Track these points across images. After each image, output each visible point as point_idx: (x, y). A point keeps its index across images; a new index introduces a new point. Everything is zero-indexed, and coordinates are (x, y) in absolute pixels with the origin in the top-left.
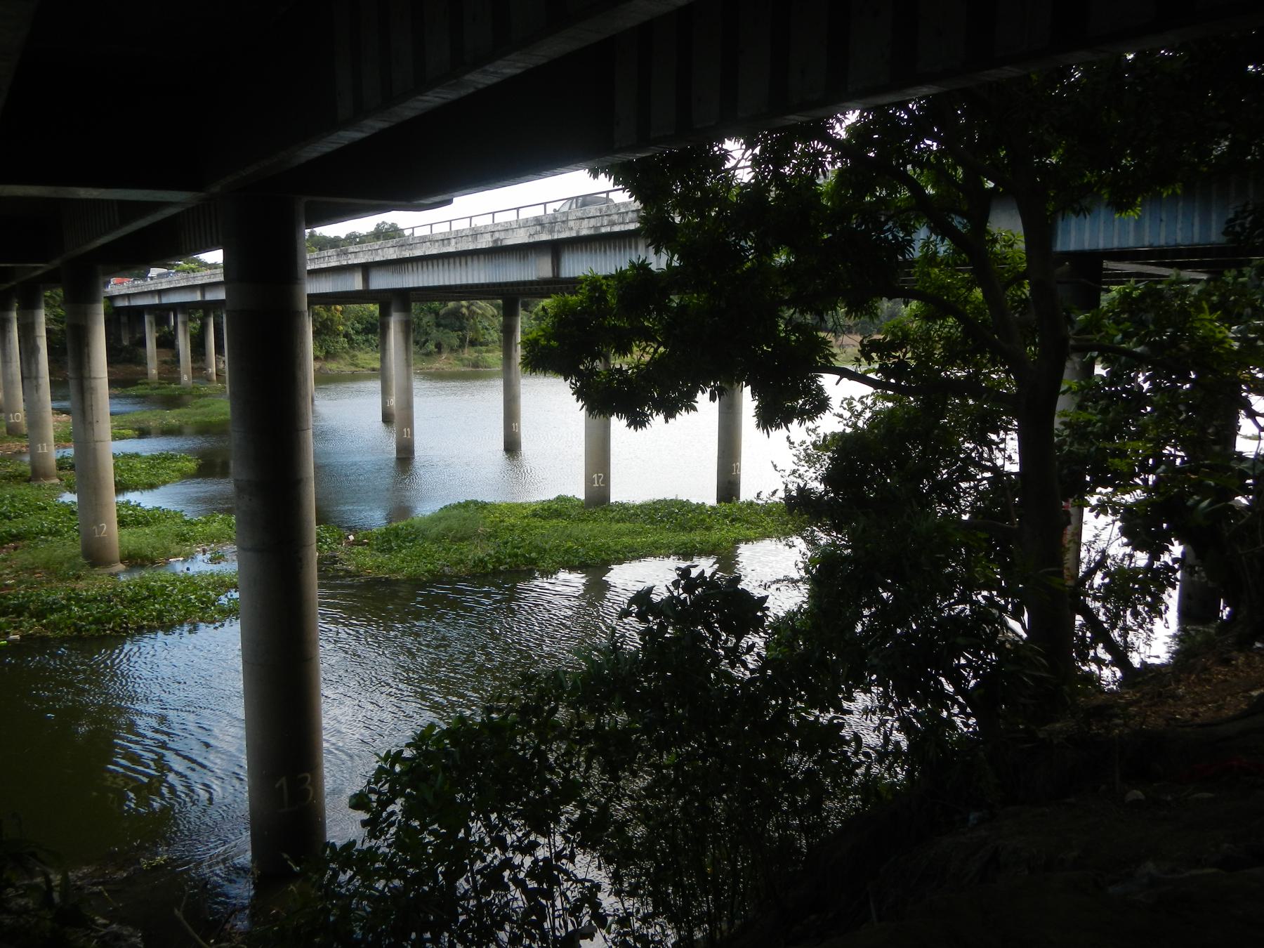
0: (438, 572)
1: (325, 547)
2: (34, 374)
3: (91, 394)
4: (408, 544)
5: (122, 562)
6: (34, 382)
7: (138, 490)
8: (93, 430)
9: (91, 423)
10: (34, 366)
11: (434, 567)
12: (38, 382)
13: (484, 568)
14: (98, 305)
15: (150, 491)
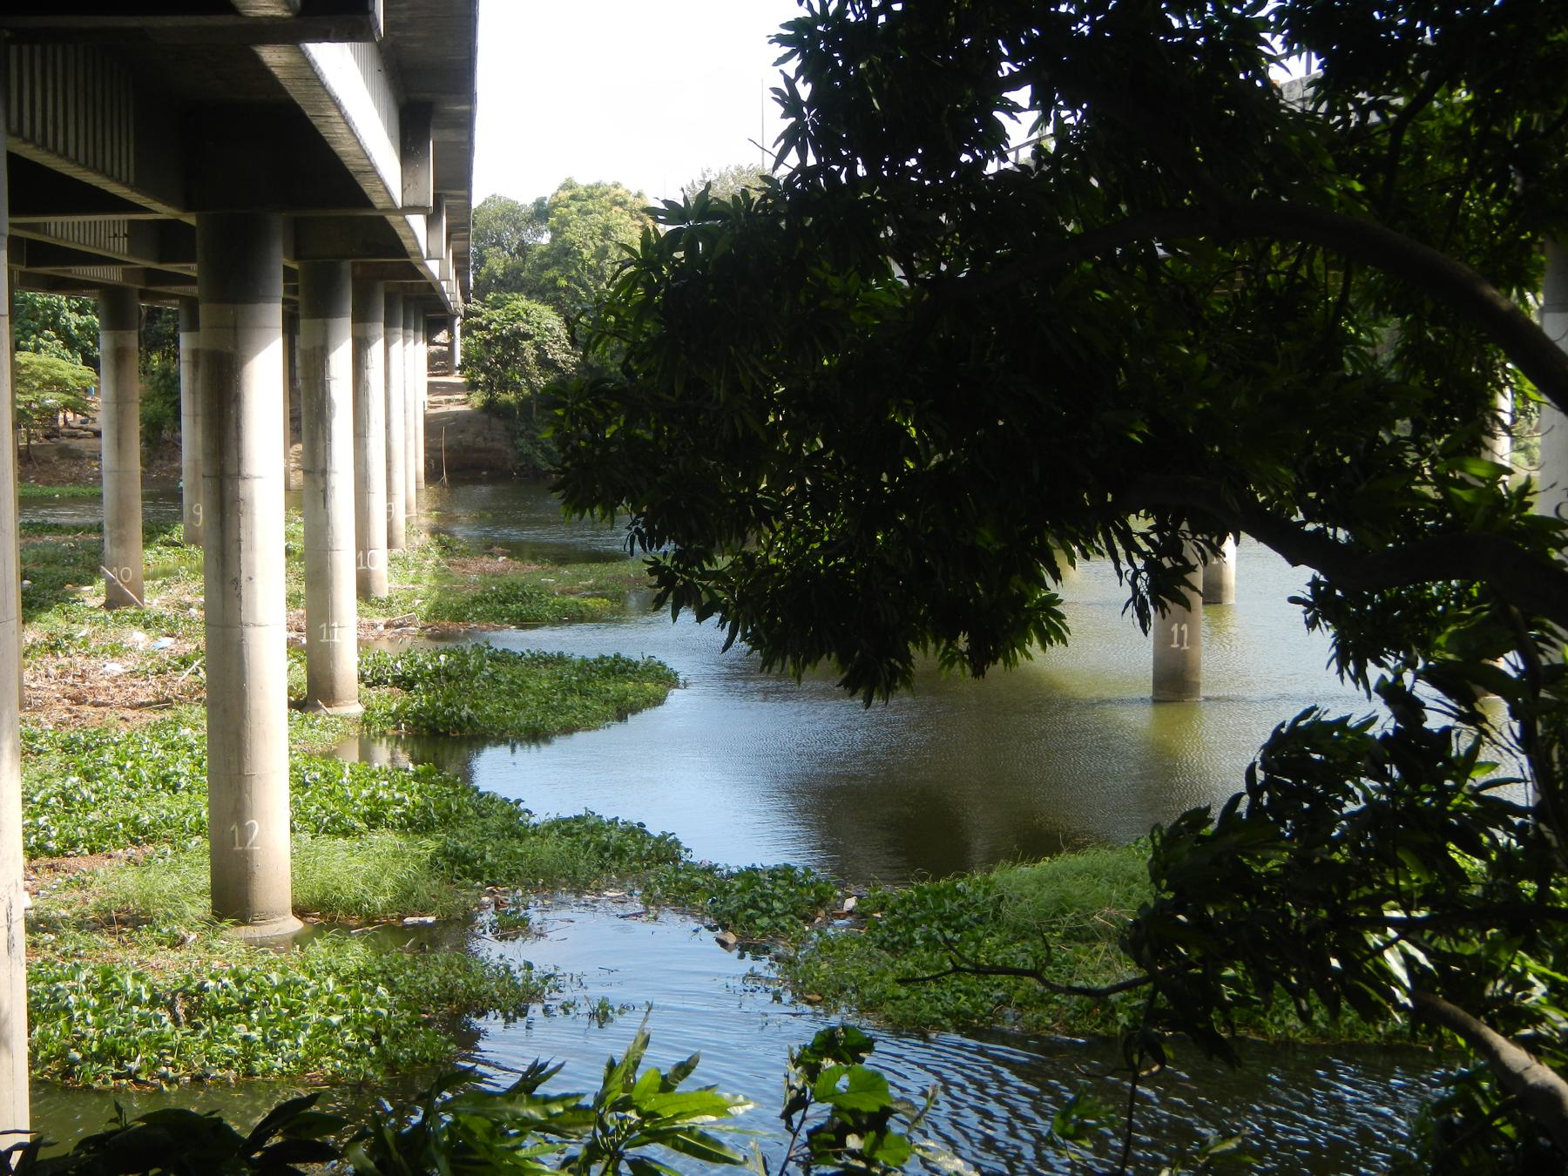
0: (981, 1019)
1: (764, 921)
2: (321, 466)
3: (238, 513)
4: (949, 934)
5: (300, 911)
6: (321, 481)
7: (506, 742)
8: (239, 596)
9: (236, 582)
10: (321, 444)
11: (974, 1006)
12: (326, 483)
13: (1105, 1021)
14: (264, 306)
15: (534, 747)
